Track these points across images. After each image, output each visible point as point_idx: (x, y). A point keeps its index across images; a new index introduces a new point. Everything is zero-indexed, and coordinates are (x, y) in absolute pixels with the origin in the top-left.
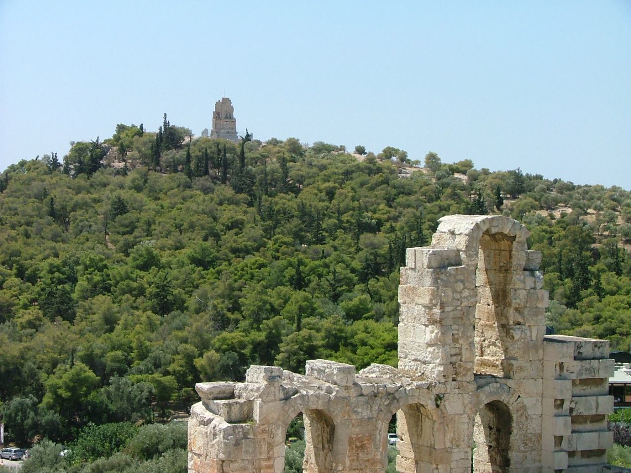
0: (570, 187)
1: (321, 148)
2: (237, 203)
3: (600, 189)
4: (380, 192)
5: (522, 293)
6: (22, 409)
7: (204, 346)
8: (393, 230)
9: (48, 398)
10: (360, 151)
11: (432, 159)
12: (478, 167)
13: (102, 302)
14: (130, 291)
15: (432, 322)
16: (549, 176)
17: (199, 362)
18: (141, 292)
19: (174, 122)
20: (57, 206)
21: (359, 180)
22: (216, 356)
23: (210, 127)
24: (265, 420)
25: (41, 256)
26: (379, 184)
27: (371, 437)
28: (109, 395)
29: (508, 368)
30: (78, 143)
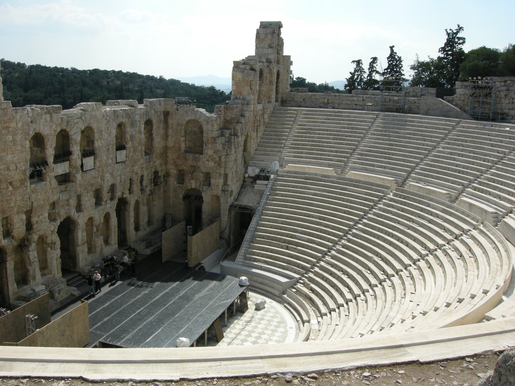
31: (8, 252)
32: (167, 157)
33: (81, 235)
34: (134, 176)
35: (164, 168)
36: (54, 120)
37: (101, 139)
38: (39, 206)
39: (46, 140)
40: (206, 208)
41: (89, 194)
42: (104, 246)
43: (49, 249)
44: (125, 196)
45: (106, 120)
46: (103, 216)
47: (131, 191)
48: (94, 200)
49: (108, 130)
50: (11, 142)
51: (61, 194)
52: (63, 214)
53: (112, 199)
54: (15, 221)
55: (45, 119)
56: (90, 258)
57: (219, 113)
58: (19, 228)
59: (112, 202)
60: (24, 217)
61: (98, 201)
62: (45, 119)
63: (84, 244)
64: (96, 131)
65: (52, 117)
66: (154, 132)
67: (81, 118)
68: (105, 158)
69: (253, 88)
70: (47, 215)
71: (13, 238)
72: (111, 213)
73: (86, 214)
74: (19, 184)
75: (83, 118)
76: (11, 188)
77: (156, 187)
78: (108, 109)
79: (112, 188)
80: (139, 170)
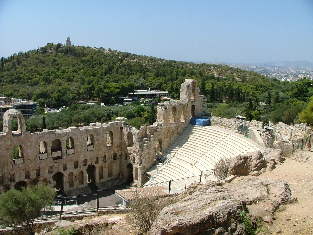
0: (136, 55)
1: (88, 47)
2: (76, 59)
3: (142, 56)
4: (102, 56)
5: (197, 90)
6: (49, 101)
7: (80, 88)
8: (106, 64)
9: (53, 99)
10: (95, 48)
11: (110, 50)
12: (118, 51)
13: (58, 80)
14: (62, 77)
15: (187, 94)
16: (132, 53)
17: (80, 91)
18: (64, 78)
19: (60, 43)
20: (42, 61)
21: (98, 54)
22: (83, 90)
23: (66, 43)
24: (169, 108)
25: (42, 71)
26: (101, 55)
27: (180, 110)
28: (65, 98)
29: (195, 100)
30: (42, 47)
31: (27, 183)
32: (122, 147)
33: (66, 179)
34: (99, 156)
35: (120, 152)
37: (77, 142)
38: (43, 168)
39: (47, 144)
40: (134, 173)
41: (70, 164)
42: (79, 184)
43: (48, 183)
44: (92, 164)
46: (78, 172)
47: (97, 162)
48: (74, 166)
50: (29, 145)
52: (55, 171)
53: (85, 165)
56: (70, 188)
57: (142, 130)
58: (33, 175)
59: (85, 167)
60: (36, 172)
63: (67, 183)
64: (74, 139)
65: (50, 135)
66: (113, 136)
67: (66, 134)
68: (80, 149)
69: (165, 117)
70: (47, 171)
71: (30, 179)
72: (83, 171)
73: (68, 171)
74: (33, 160)
75: (67, 134)
76: (29, 161)
77: (114, 160)
78: (84, 129)
79: (86, 161)
80: (102, 153)
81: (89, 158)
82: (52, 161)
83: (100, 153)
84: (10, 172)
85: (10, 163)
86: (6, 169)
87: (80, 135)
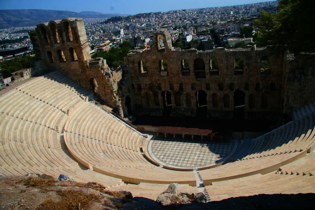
36: (192, 55)
43: (192, 98)
45: (226, 55)
47: (247, 88)
48: (218, 88)
49: (227, 60)
51: (196, 81)
54: (174, 85)
55: (188, 54)
58: (176, 87)
60: (179, 85)
61: (221, 87)
62: (188, 54)
63: (211, 102)
70: (190, 87)
71: (174, 90)
73: (211, 91)
74: (176, 75)
75: (210, 54)
76: (173, 75)
78: (231, 50)
81: (236, 82)
82: (194, 79)
83: (252, 80)
84: (157, 82)
85: (157, 74)
86: (154, 78)
87: (225, 56)
